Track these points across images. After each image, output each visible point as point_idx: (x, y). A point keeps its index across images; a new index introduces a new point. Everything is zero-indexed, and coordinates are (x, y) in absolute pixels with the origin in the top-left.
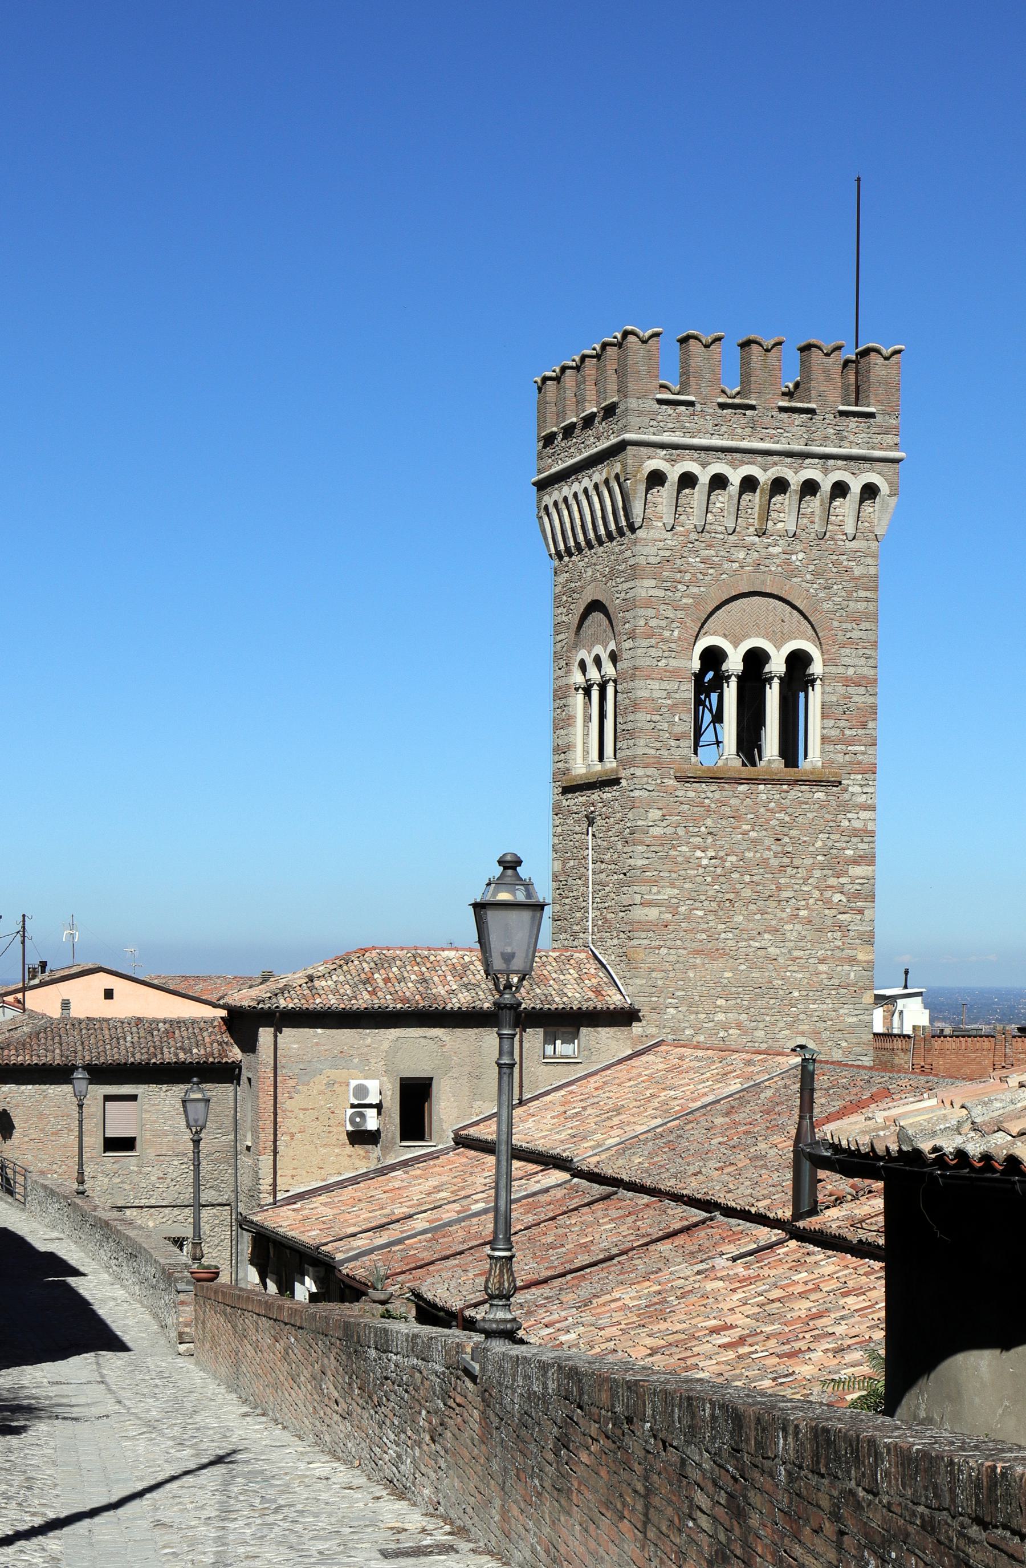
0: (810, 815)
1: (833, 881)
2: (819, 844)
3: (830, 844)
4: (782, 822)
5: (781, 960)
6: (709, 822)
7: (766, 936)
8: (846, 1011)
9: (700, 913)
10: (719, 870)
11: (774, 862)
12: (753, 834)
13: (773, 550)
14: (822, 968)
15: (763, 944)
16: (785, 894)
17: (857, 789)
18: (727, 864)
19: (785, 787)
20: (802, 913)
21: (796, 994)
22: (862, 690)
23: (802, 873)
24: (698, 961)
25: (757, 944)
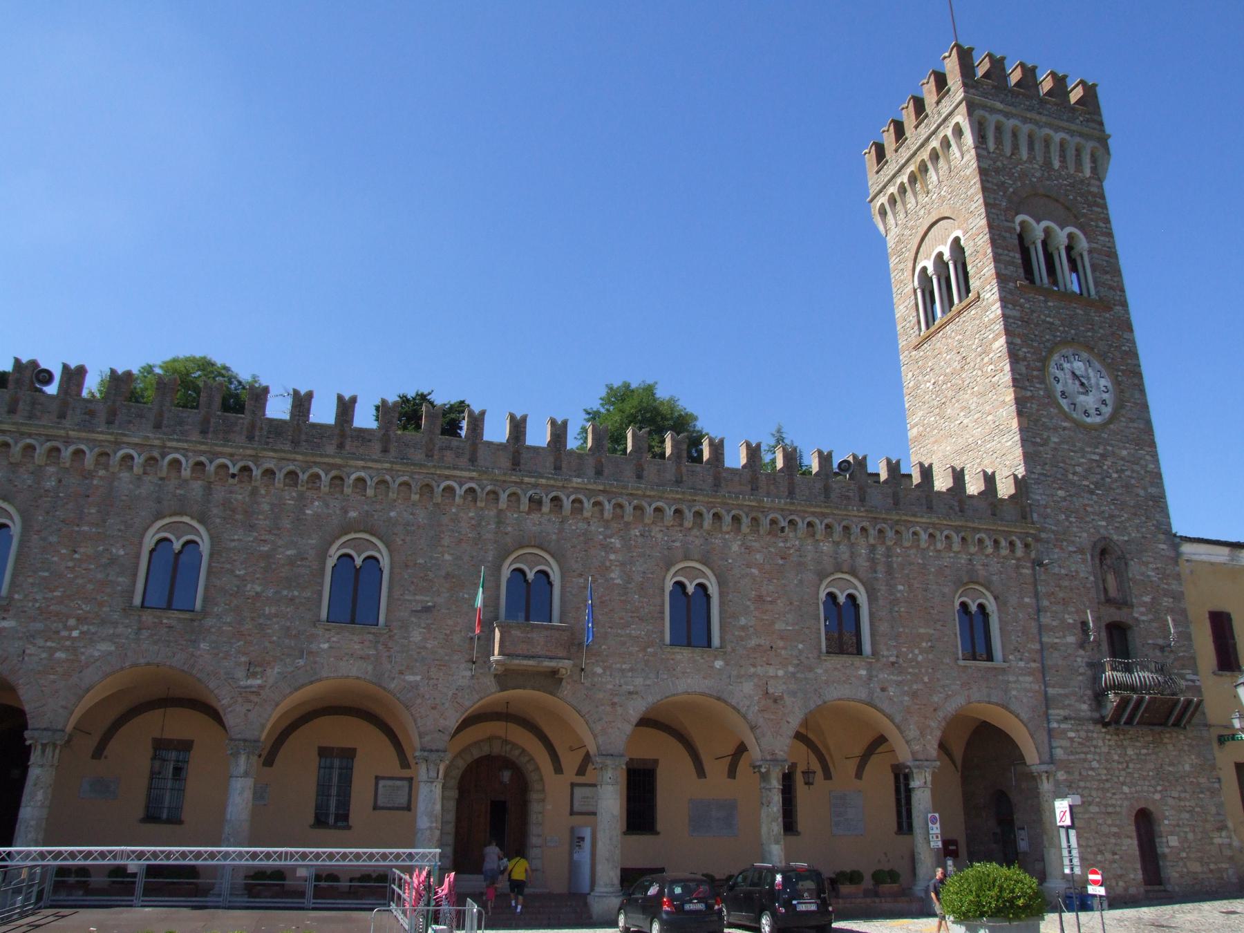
0: (970, 328)
1: (986, 360)
2: (977, 340)
3: (981, 338)
4: (960, 342)
5: (970, 425)
6: (930, 364)
7: (962, 414)
8: (1005, 440)
9: (933, 419)
10: (937, 389)
11: (959, 367)
12: (948, 357)
13: (934, 197)
14: (990, 418)
15: (962, 419)
16: (966, 383)
17: (989, 294)
18: (940, 382)
19: (957, 320)
20: (976, 389)
21: (979, 442)
22: (981, 236)
23: (972, 364)
24: (935, 448)
25: (959, 422)
